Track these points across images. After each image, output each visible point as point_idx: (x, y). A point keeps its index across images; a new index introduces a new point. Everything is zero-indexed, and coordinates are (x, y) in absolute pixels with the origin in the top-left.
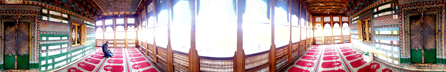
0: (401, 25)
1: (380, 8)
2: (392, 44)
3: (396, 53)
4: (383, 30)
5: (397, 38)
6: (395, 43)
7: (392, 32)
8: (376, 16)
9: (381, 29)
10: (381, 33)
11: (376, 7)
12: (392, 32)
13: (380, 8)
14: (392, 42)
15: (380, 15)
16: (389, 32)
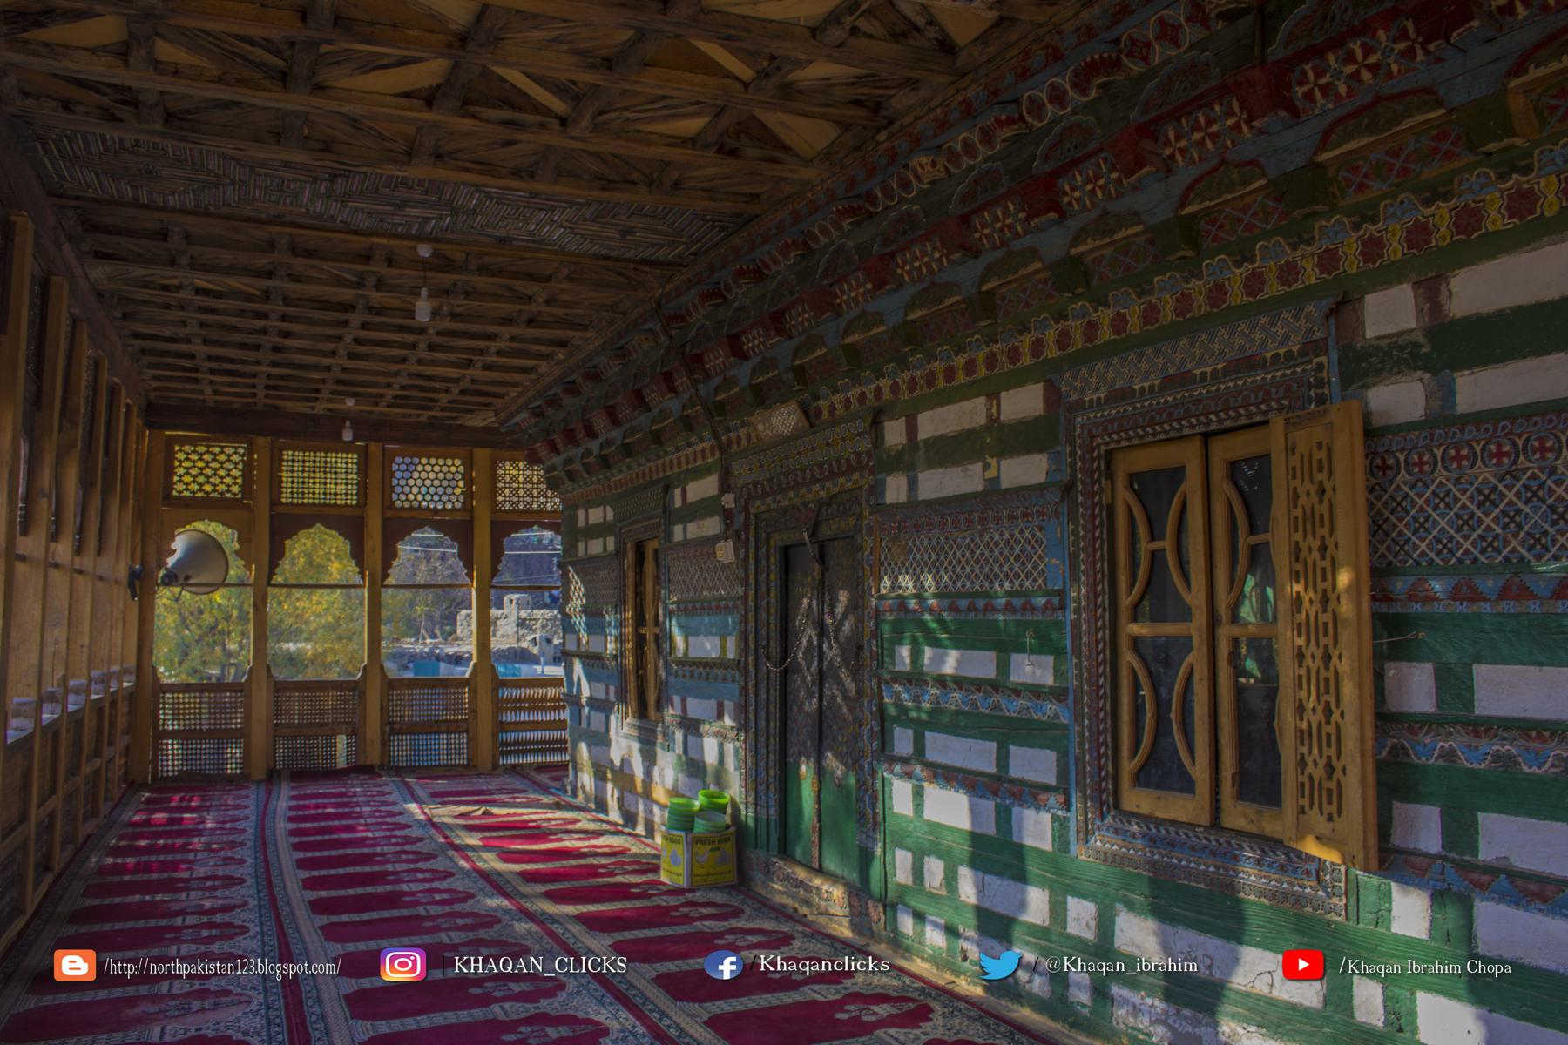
11: (679, 474)
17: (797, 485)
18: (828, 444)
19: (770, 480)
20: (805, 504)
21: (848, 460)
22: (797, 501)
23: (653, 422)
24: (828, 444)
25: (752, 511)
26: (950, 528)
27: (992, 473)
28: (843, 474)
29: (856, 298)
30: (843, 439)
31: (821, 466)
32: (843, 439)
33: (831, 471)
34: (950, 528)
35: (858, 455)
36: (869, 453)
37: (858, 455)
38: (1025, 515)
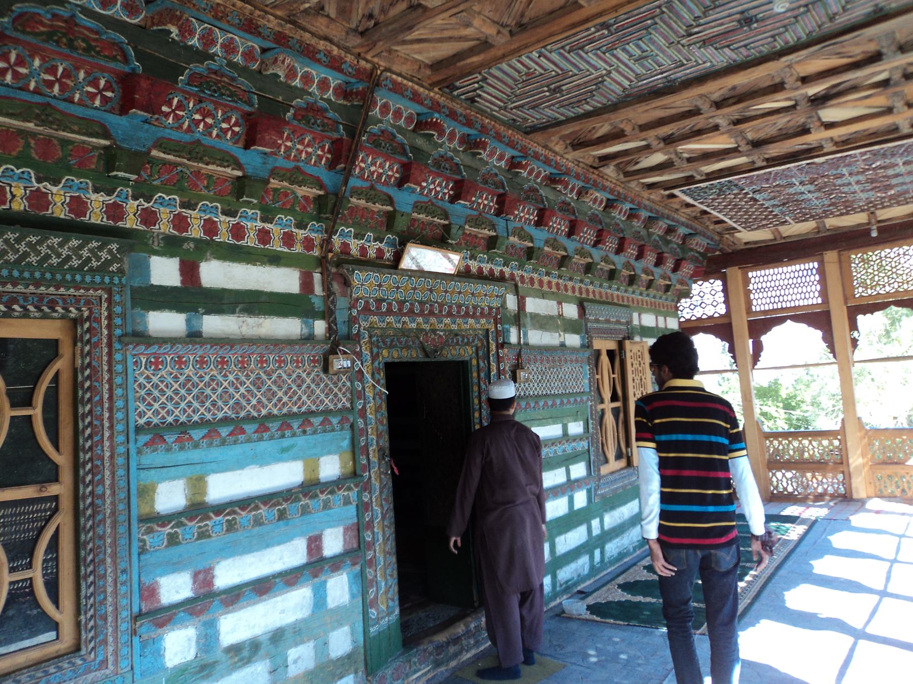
0: (363, 413)
1: (215, 274)
2: (317, 566)
3: (339, 616)
4: (240, 464)
5: (347, 502)
6: (333, 543)
7: (312, 466)
8: (165, 322)
9: (216, 453)
10: (222, 487)
12: (312, 466)
13: (215, 274)
14: (315, 544)
15: (214, 324)
16: (286, 474)
17: (431, 313)
18: (473, 294)
19: (401, 303)
20: (434, 331)
21: (467, 308)
22: (426, 327)
23: (161, 144)
24: (473, 294)
25: (364, 324)
26: (545, 362)
27: (562, 339)
28: (473, 316)
29: (521, 218)
30: (486, 295)
31: (459, 306)
32: (486, 295)
33: (467, 313)
34: (545, 362)
35: (490, 308)
36: (498, 309)
37: (490, 308)
38: (577, 361)
